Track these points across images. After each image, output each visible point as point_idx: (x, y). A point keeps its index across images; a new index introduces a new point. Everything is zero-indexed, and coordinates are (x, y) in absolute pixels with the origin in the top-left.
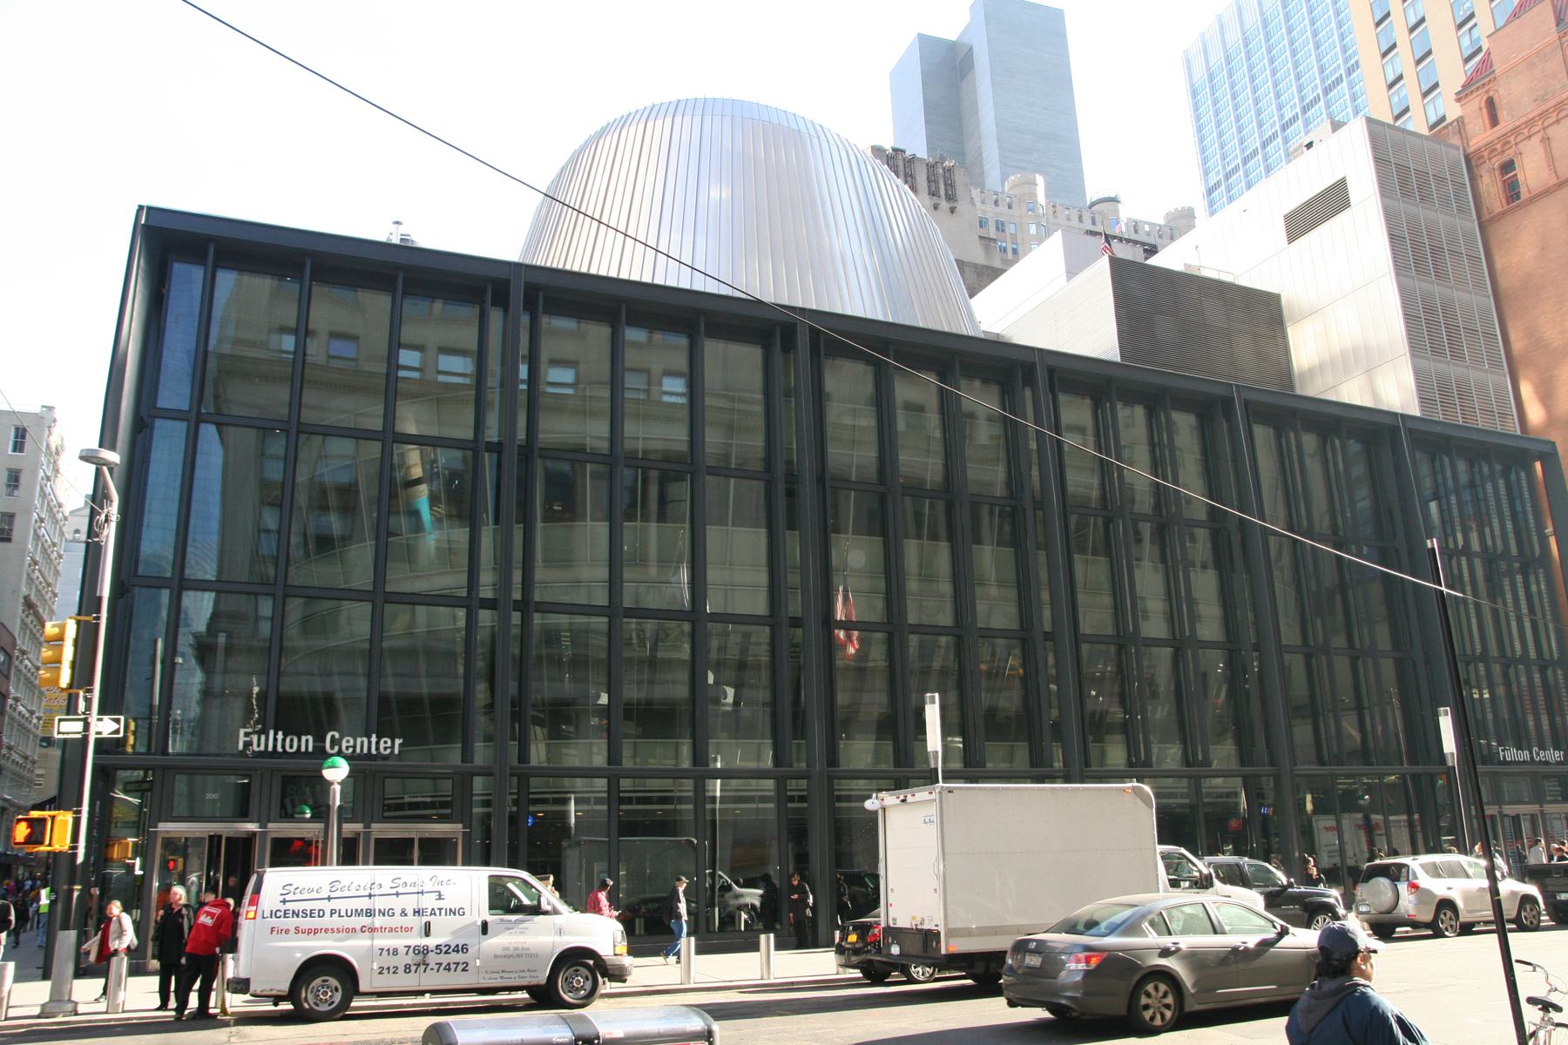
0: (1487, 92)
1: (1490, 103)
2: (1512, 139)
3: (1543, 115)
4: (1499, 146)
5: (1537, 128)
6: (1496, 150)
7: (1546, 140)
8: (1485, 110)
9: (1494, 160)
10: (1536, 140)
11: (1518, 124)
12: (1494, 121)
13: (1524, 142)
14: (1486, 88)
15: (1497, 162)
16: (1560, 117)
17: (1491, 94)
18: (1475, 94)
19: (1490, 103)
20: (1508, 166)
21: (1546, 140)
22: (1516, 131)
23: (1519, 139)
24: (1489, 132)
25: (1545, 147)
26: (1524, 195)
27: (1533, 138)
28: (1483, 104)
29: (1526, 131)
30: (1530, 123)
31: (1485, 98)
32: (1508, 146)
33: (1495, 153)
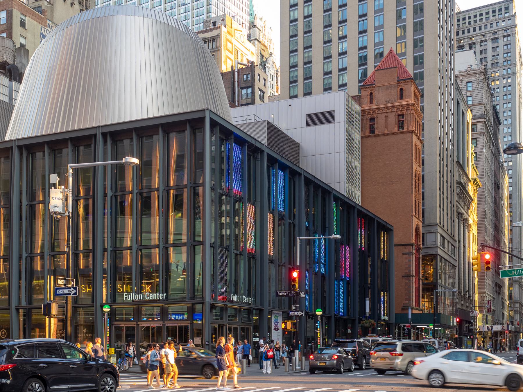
0: (371, 90)
1: (371, 94)
2: (376, 111)
3: (388, 108)
4: (371, 112)
5: (384, 112)
6: (370, 113)
7: (386, 117)
8: (369, 96)
9: (369, 116)
10: (385, 114)
11: (379, 107)
12: (371, 102)
13: (380, 114)
14: (371, 89)
15: (369, 116)
16: (393, 111)
17: (372, 92)
18: (367, 89)
19: (371, 94)
20: (372, 119)
21: (386, 117)
22: (378, 109)
23: (379, 112)
24: (369, 105)
25: (386, 119)
26: (376, 133)
27: (383, 114)
28: (369, 94)
29: (381, 111)
30: (383, 108)
31: (370, 92)
32: (374, 113)
33: (369, 114)
